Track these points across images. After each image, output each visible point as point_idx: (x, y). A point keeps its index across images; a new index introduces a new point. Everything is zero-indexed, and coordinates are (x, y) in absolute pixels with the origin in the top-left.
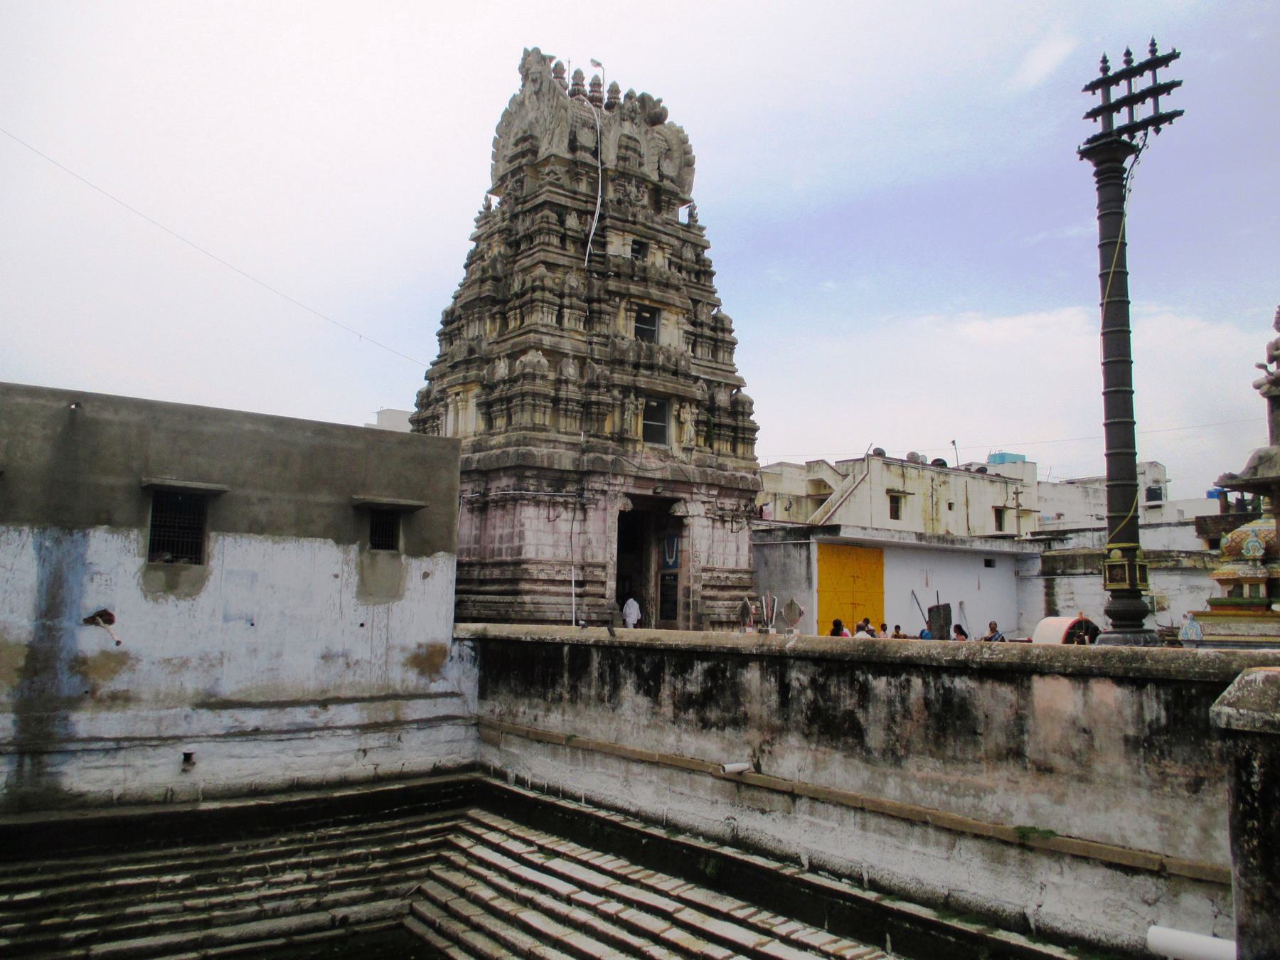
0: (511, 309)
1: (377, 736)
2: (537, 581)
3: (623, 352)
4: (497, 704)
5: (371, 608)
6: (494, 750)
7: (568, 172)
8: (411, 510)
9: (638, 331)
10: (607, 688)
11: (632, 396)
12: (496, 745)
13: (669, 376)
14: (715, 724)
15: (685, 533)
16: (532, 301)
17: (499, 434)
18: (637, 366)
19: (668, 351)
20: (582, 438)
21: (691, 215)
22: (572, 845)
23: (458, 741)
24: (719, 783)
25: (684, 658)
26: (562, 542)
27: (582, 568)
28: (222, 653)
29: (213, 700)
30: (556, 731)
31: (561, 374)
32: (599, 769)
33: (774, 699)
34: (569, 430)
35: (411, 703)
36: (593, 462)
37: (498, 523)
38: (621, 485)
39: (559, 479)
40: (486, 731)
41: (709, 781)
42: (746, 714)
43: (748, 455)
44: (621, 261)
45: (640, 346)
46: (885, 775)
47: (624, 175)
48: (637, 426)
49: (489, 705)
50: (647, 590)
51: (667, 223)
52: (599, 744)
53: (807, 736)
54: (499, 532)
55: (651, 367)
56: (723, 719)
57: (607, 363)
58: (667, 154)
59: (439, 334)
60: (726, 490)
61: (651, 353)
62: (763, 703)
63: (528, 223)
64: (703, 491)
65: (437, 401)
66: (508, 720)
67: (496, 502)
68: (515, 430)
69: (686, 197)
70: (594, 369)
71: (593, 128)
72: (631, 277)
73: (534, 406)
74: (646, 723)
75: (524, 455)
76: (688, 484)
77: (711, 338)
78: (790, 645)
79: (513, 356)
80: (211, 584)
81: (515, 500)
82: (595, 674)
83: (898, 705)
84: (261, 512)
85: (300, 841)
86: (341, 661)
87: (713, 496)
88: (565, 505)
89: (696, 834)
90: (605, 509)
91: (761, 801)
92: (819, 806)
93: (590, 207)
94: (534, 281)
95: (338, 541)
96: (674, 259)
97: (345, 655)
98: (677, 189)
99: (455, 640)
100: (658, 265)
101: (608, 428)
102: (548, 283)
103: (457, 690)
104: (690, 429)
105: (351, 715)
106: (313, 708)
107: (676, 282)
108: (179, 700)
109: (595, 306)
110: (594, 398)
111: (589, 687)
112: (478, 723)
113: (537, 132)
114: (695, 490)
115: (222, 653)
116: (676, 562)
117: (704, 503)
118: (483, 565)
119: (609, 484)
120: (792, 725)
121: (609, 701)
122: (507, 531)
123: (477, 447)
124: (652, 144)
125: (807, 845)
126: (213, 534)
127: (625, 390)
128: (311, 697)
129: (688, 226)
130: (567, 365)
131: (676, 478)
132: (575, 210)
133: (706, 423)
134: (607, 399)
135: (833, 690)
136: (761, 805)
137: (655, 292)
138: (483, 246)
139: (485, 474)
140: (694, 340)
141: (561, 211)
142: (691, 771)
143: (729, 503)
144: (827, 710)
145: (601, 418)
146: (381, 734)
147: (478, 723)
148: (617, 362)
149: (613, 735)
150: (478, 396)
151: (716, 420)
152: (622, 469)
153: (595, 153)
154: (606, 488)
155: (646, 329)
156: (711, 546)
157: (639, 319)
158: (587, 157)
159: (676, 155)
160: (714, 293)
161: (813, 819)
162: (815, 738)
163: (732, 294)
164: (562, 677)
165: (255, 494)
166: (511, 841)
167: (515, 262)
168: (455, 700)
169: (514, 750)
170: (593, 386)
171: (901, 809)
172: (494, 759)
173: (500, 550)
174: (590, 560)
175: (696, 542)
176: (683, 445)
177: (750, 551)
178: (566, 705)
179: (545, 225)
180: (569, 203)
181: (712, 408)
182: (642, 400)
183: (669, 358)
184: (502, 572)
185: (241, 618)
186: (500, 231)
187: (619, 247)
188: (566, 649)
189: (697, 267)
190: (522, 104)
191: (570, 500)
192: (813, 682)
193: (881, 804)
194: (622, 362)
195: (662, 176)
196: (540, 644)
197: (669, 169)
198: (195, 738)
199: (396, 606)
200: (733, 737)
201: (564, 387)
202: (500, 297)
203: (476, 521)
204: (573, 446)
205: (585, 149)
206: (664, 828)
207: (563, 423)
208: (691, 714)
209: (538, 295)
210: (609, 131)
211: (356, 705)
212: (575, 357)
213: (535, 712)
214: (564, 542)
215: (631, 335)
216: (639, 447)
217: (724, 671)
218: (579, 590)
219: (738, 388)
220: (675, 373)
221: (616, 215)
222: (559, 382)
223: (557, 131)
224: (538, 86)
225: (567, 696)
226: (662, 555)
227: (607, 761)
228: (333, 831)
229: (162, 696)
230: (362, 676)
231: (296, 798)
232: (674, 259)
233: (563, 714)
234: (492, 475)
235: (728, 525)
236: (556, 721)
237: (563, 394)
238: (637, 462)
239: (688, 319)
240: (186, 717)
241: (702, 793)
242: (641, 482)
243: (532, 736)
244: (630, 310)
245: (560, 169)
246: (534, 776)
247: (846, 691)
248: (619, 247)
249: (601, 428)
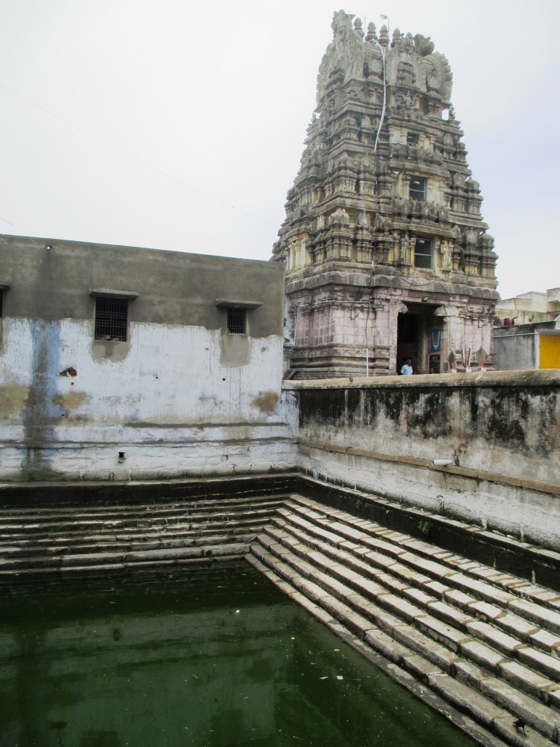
0: (326, 184)
1: (234, 447)
2: (343, 358)
3: (400, 208)
4: (309, 430)
5: (229, 369)
6: (307, 459)
7: (363, 90)
9: (411, 194)
10: (369, 415)
11: (407, 236)
12: (307, 454)
13: (433, 223)
14: (432, 435)
15: (445, 328)
16: (339, 177)
17: (319, 265)
18: (410, 217)
19: (432, 206)
20: (372, 265)
21: (451, 115)
22: (347, 515)
23: (286, 453)
24: (433, 473)
25: (414, 392)
26: (362, 336)
27: (374, 350)
28: (140, 395)
29: (135, 422)
30: (341, 445)
31: (358, 224)
32: (364, 468)
33: (468, 416)
34: (364, 260)
35: (255, 428)
36: (379, 280)
37: (320, 322)
38: (399, 296)
39: (357, 292)
40: (303, 447)
41: (427, 472)
42: (450, 427)
43: (490, 276)
44: (398, 147)
45: (412, 204)
46: (538, 464)
47: (402, 89)
48: (410, 257)
49: (305, 431)
50: (420, 366)
51: (432, 120)
52: (363, 451)
53: (488, 440)
54: (320, 327)
55: (420, 217)
56: (436, 431)
57: (390, 215)
58: (433, 72)
59: (286, 206)
60: (473, 299)
61: (420, 208)
62: (462, 419)
63: (337, 127)
64: (457, 299)
65: (284, 247)
66: (315, 439)
67: (318, 308)
68: (328, 261)
69: (447, 102)
70: (380, 220)
71: (380, 59)
72: (406, 158)
73: (340, 245)
74: (391, 436)
75: (333, 277)
76: (446, 295)
77: (464, 197)
78: (478, 379)
79: (327, 214)
80: (132, 353)
81: (329, 306)
82: (363, 407)
83: (547, 415)
84: (159, 310)
85: (187, 506)
86: (212, 401)
87: (464, 303)
88: (362, 309)
89: (419, 507)
90: (388, 312)
91: (458, 484)
92: (494, 486)
93: (377, 112)
94: (340, 163)
95: (208, 327)
96: (437, 144)
97: (214, 398)
98: (439, 96)
99: (283, 390)
100: (425, 148)
101: (390, 259)
102: (349, 164)
103: (285, 422)
104: (448, 258)
105: (218, 434)
106: (195, 429)
107: (438, 159)
108: (115, 421)
109: (382, 178)
110: (380, 239)
111: (359, 416)
112: (298, 442)
113: (343, 67)
114: (451, 299)
115: (140, 395)
116: (439, 347)
117: (458, 307)
118: (311, 349)
119: (391, 295)
120: (479, 432)
121: (370, 424)
122: (325, 326)
123: (307, 274)
124: (422, 67)
125: (486, 513)
126: (132, 323)
127: (402, 233)
128: (193, 422)
129: (448, 122)
130: (362, 218)
131: (438, 291)
132: (368, 115)
133: (460, 254)
134: (389, 239)
135: (505, 407)
136: (458, 487)
137: (423, 167)
138: (311, 145)
139: (312, 291)
140: (451, 199)
141: (359, 116)
142: (417, 466)
143: (476, 308)
144: (501, 421)
145: (386, 251)
146: (237, 447)
147: (298, 442)
149: (372, 445)
150: (306, 242)
151: (467, 252)
152: (400, 285)
153: (381, 76)
154: (389, 297)
156: (462, 334)
157: (412, 186)
158: (376, 80)
159: (439, 73)
160: (467, 166)
161: (489, 495)
162: (493, 441)
163: (479, 165)
164: (344, 410)
165: (156, 299)
166: (312, 512)
167: (329, 153)
168: (284, 428)
169: (318, 458)
170: (380, 231)
171: (546, 486)
172: (307, 465)
173: (321, 338)
174: (378, 345)
175: (452, 334)
176: (443, 269)
177: (491, 341)
178: (346, 428)
179: (347, 126)
180: (364, 110)
181: (464, 245)
182: (414, 239)
183: (432, 211)
184: (322, 353)
185: (149, 374)
186: (320, 134)
187: (398, 138)
188: (346, 392)
189: (454, 149)
190: (334, 49)
191: (365, 305)
192: (493, 402)
193: (533, 483)
194: (399, 215)
195: (429, 89)
196: (331, 390)
197: (434, 83)
198: (125, 444)
199: (245, 368)
200: (442, 444)
201: (360, 232)
202: (320, 176)
203: (307, 321)
204: (367, 270)
206: (401, 503)
208: (418, 430)
209: (342, 172)
210: (391, 60)
211: (221, 428)
212: (367, 212)
213: (329, 434)
214: (362, 333)
215: (407, 197)
216: (411, 270)
217: (438, 398)
218: (371, 364)
219: (484, 230)
220: (437, 221)
222: (357, 229)
223: (355, 64)
224: (343, 35)
225: (347, 422)
226: (431, 343)
227: (369, 462)
228: (207, 502)
229: (105, 419)
230: (225, 411)
231: (185, 481)
232: (437, 144)
233: (345, 434)
234: (316, 291)
235: (476, 323)
236: (340, 438)
237: (359, 237)
238: (410, 280)
239: (447, 184)
240: (120, 431)
241: (423, 480)
242: (413, 294)
243: (327, 448)
244: (406, 180)
245: (358, 89)
246: (329, 473)
247: (513, 407)
248: (398, 138)
249: (386, 258)
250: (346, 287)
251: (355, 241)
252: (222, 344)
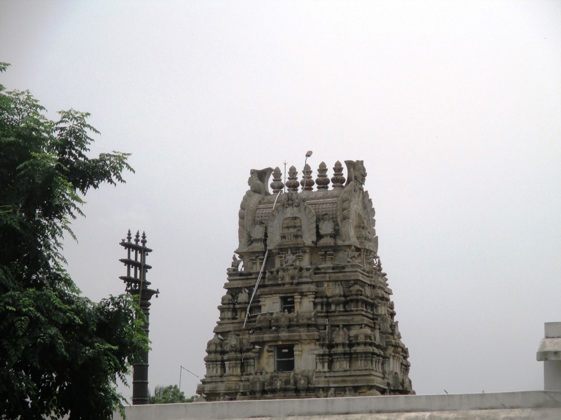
72: (270, 327)
77: (345, 354)
96: (318, 300)
109: (244, 355)
137: (284, 334)
140: (329, 358)
157: (280, 355)
158: (258, 246)
187: (271, 305)
205: (257, 240)
221: (270, 283)
232: (318, 300)
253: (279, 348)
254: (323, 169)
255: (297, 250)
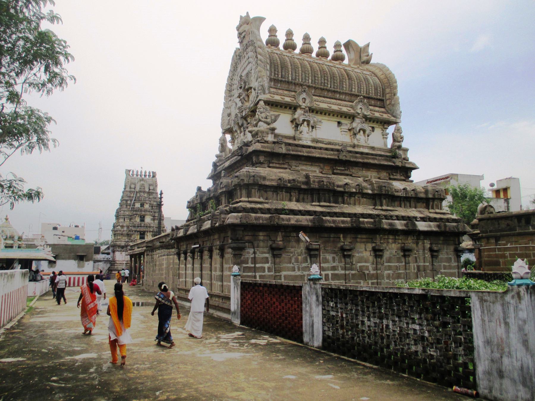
8: (85, 256)
39: (123, 247)
84: (63, 257)
95: (75, 260)
127: (135, 231)
141: (127, 201)
145: (131, 236)
148: (134, 227)
155: (142, 219)
157: (141, 218)
158: (133, 190)
187: (138, 205)
207: (124, 238)
250: (119, 246)
251: (122, 234)
252: (78, 264)
253: (141, 216)
254: (145, 172)
255: (144, 192)
